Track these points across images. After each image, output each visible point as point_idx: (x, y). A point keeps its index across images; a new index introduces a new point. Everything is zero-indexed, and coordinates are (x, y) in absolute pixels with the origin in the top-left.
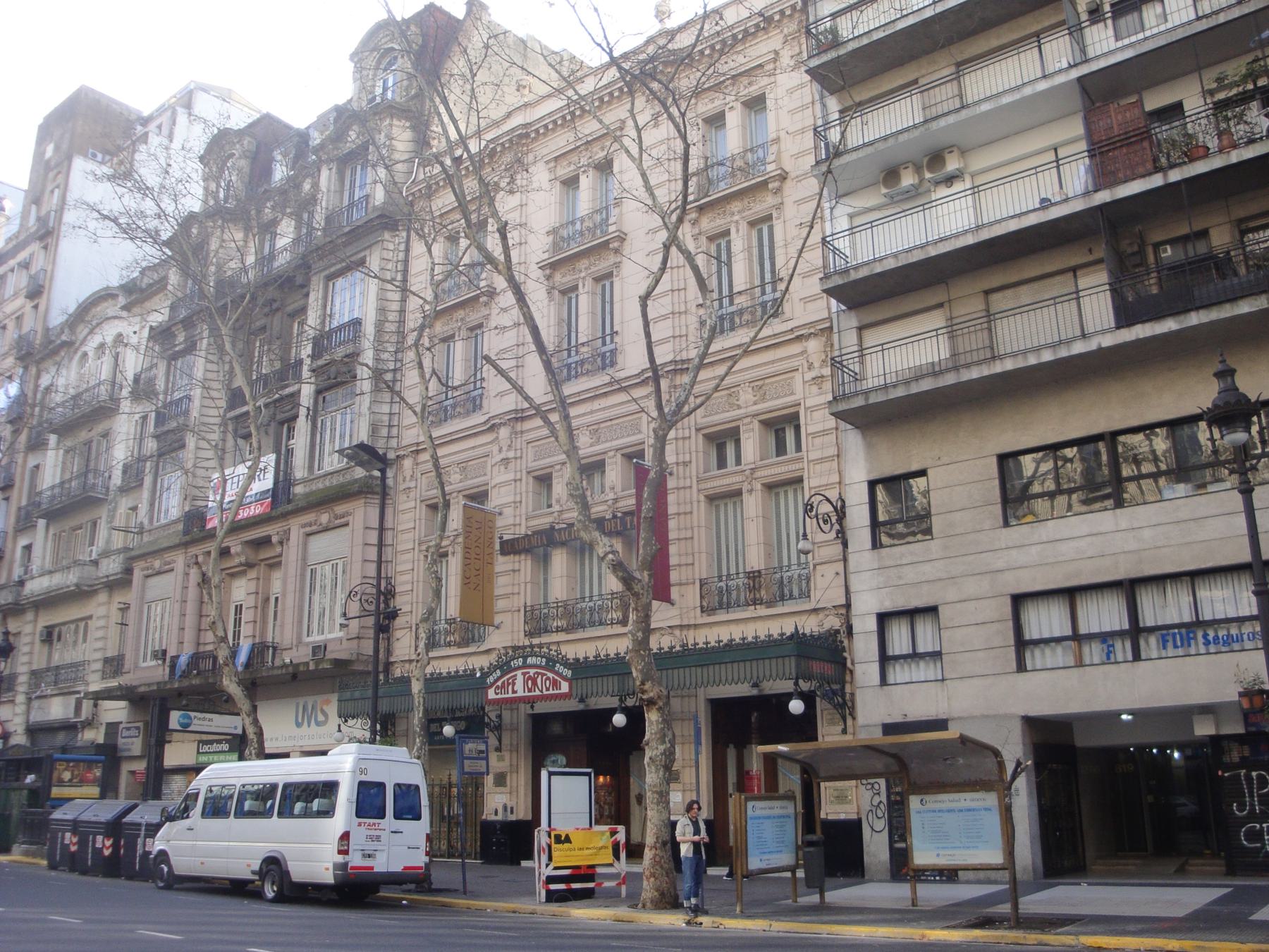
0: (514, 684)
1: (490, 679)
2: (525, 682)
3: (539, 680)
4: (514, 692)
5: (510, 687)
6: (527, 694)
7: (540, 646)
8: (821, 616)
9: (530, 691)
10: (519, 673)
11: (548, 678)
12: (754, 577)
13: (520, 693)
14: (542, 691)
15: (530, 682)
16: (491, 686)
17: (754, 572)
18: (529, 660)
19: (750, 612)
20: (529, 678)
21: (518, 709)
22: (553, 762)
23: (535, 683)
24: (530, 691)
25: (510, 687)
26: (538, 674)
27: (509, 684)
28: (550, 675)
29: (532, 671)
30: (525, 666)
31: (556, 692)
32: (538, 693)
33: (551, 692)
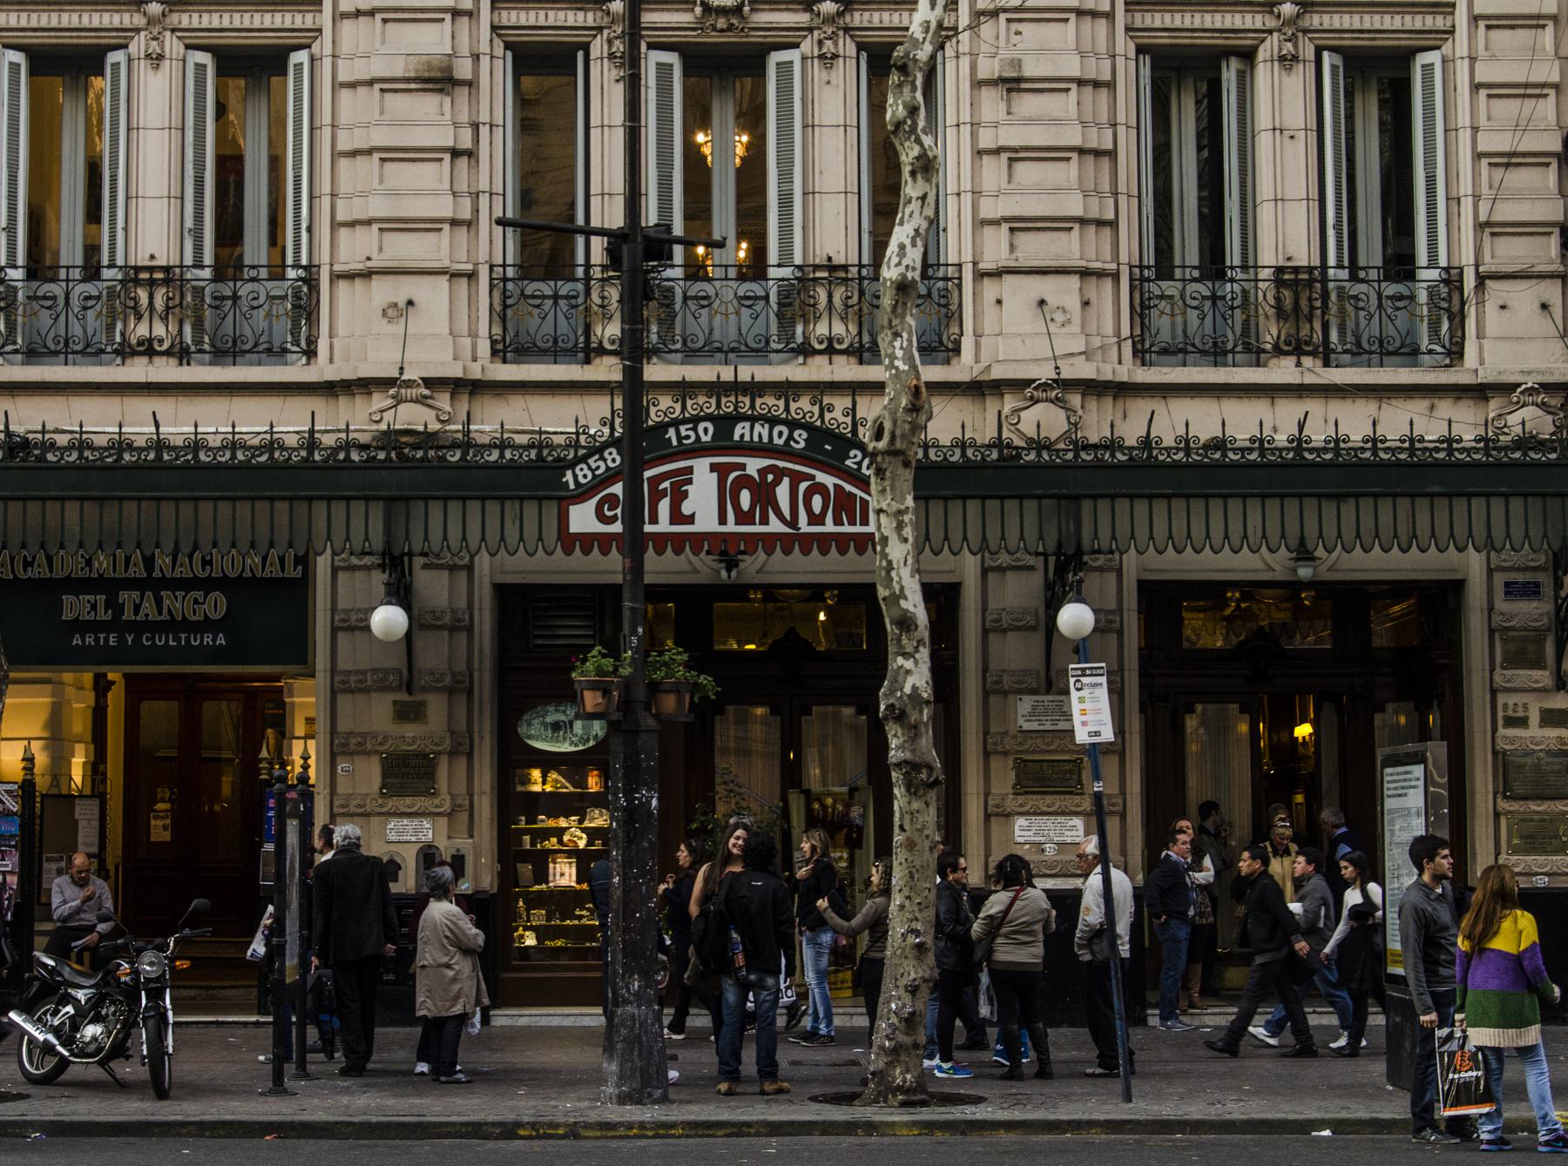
0: (679, 496)
1: (583, 474)
2: (728, 495)
3: (783, 492)
4: (677, 517)
5: (664, 506)
6: (731, 527)
7: (788, 389)
8: (1494, 406)
9: (743, 518)
10: (701, 467)
11: (821, 489)
12: (1297, 282)
13: (706, 522)
14: (793, 523)
15: (745, 498)
16: (582, 494)
17: (1296, 270)
18: (741, 430)
19: (1283, 371)
20: (745, 481)
21: (470, 568)
22: (556, 727)
23: (764, 495)
24: (743, 518)
25: (664, 506)
26: (780, 473)
27: (657, 496)
28: (829, 481)
29: (753, 465)
30: (723, 443)
31: (847, 529)
32: (775, 526)
33: (829, 527)
